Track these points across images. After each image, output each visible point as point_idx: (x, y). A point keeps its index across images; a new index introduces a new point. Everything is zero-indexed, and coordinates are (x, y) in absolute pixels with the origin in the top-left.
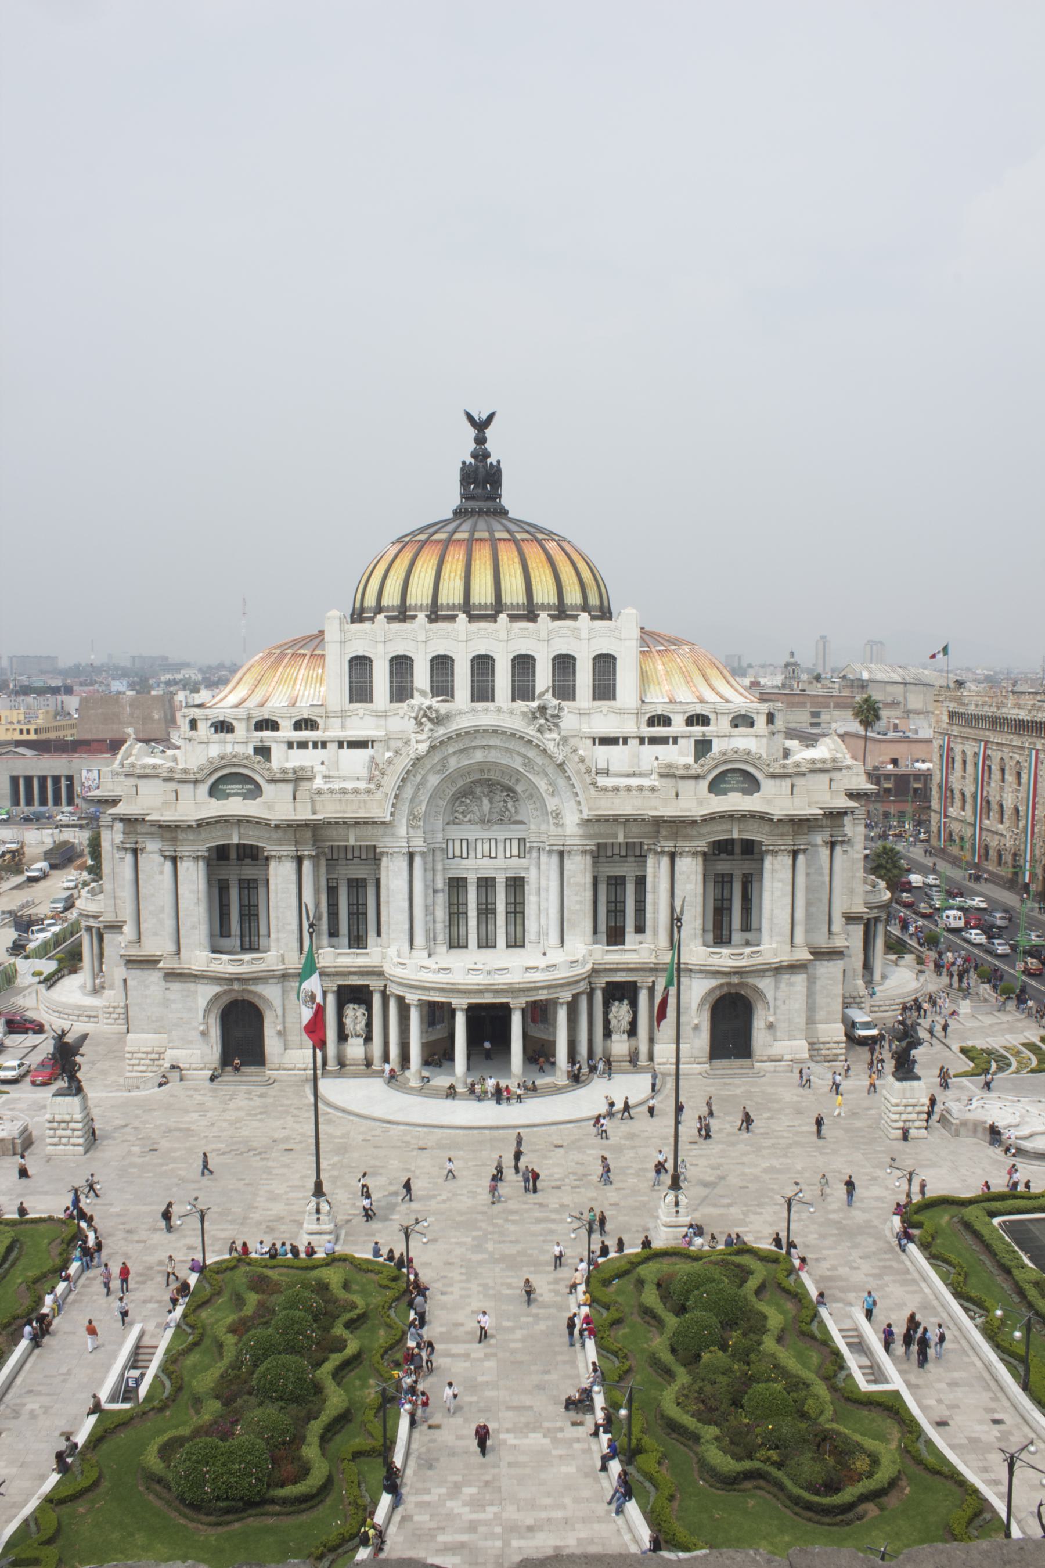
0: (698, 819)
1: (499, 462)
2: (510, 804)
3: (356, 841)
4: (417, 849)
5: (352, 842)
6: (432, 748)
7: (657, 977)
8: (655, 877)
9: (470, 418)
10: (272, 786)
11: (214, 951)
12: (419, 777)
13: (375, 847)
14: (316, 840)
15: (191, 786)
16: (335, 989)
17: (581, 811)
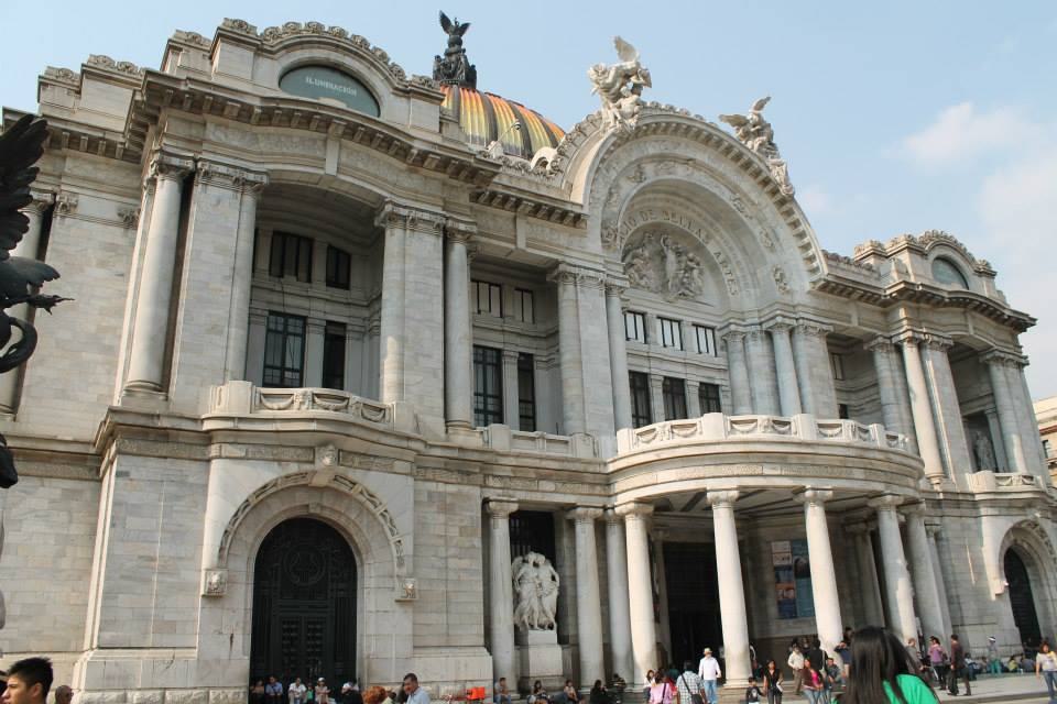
0: (946, 295)
1: (473, 66)
2: (695, 272)
3: (528, 245)
6: (638, 128)
8: (894, 383)
9: (445, 21)
10: (401, 103)
11: (265, 385)
12: (613, 174)
13: (557, 263)
15: (250, 54)
16: (514, 507)
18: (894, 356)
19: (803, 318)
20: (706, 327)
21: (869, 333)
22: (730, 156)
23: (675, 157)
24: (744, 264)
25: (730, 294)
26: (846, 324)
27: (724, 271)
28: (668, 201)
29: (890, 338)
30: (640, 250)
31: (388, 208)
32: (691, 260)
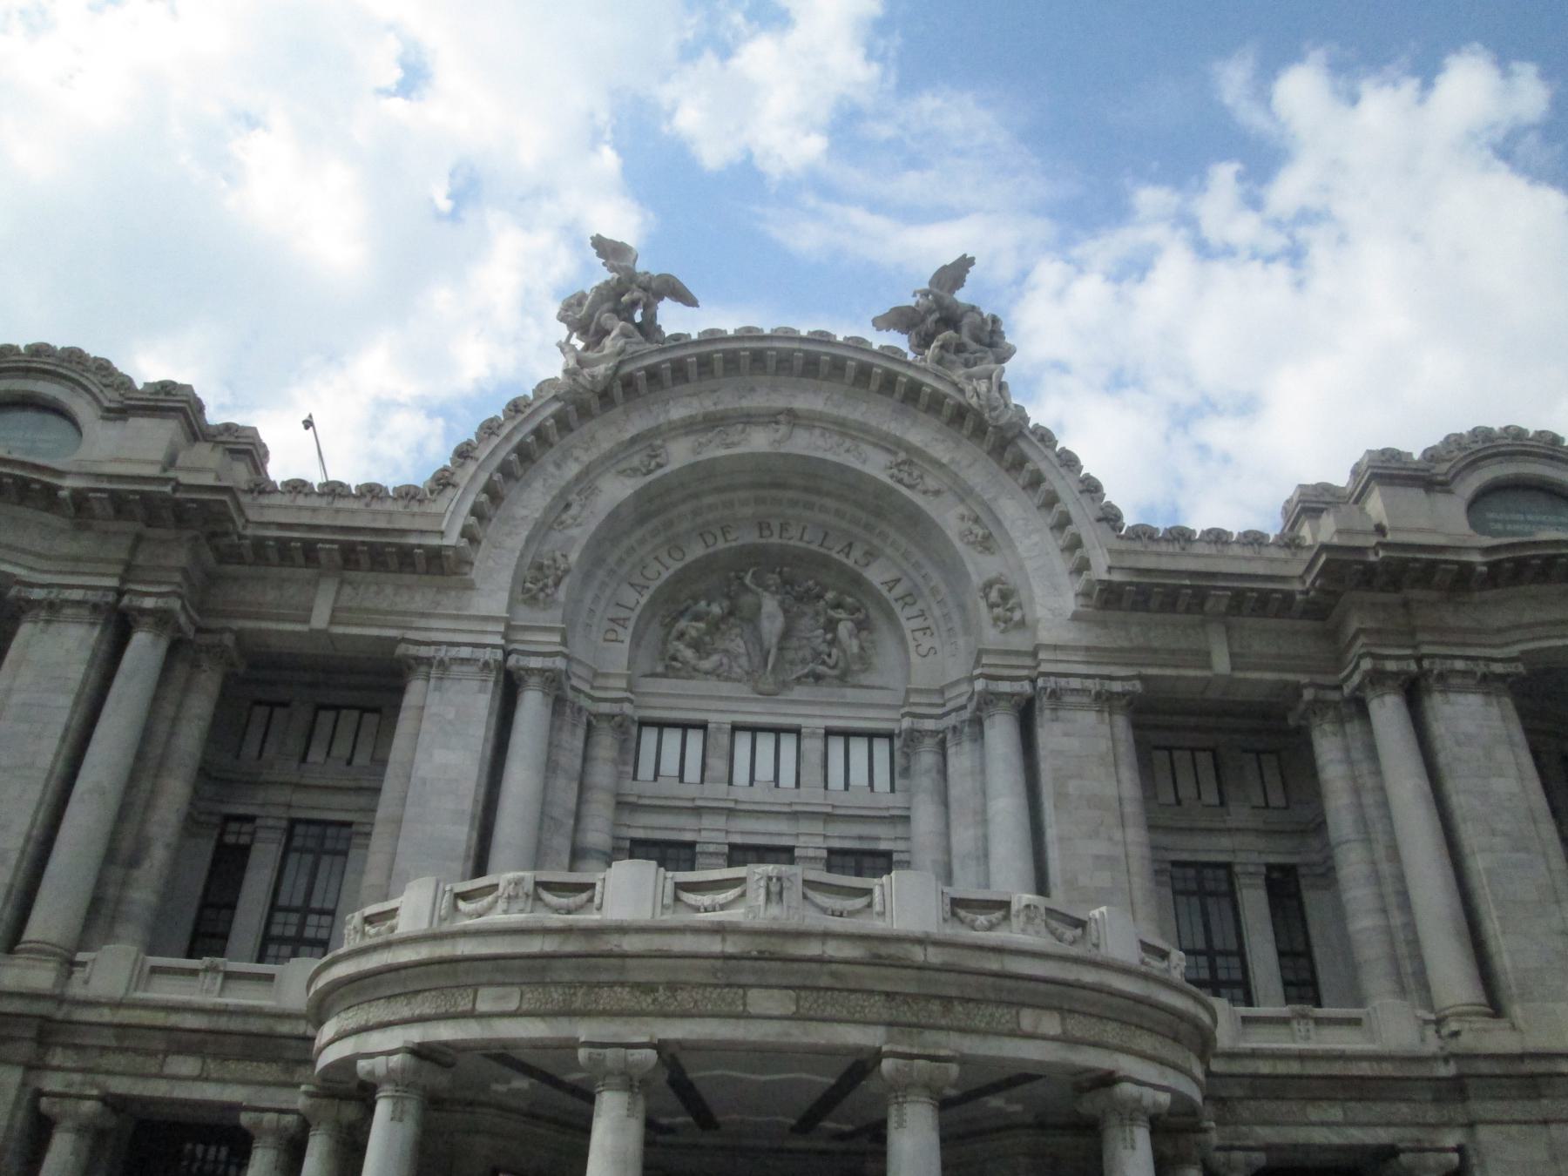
0: (1476, 558)
2: (844, 629)
3: (333, 621)
4: (535, 663)
5: (320, 619)
7: (1471, 1125)
8: (1357, 791)
14: (203, 588)
16: (88, 1107)
17: (1082, 567)
18: (1353, 728)
19: (1047, 674)
20: (871, 736)
21: (1286, 684)
22: (874, 386)
23: (749, 415)
24: (943, 588)
25: (914, 658)
26: (1191, 673)
27: (902, 614)
28: (759, 501)
29: (1339, 688)
30: (703, 603)
31: (13, 592)
32: (838, 605)
